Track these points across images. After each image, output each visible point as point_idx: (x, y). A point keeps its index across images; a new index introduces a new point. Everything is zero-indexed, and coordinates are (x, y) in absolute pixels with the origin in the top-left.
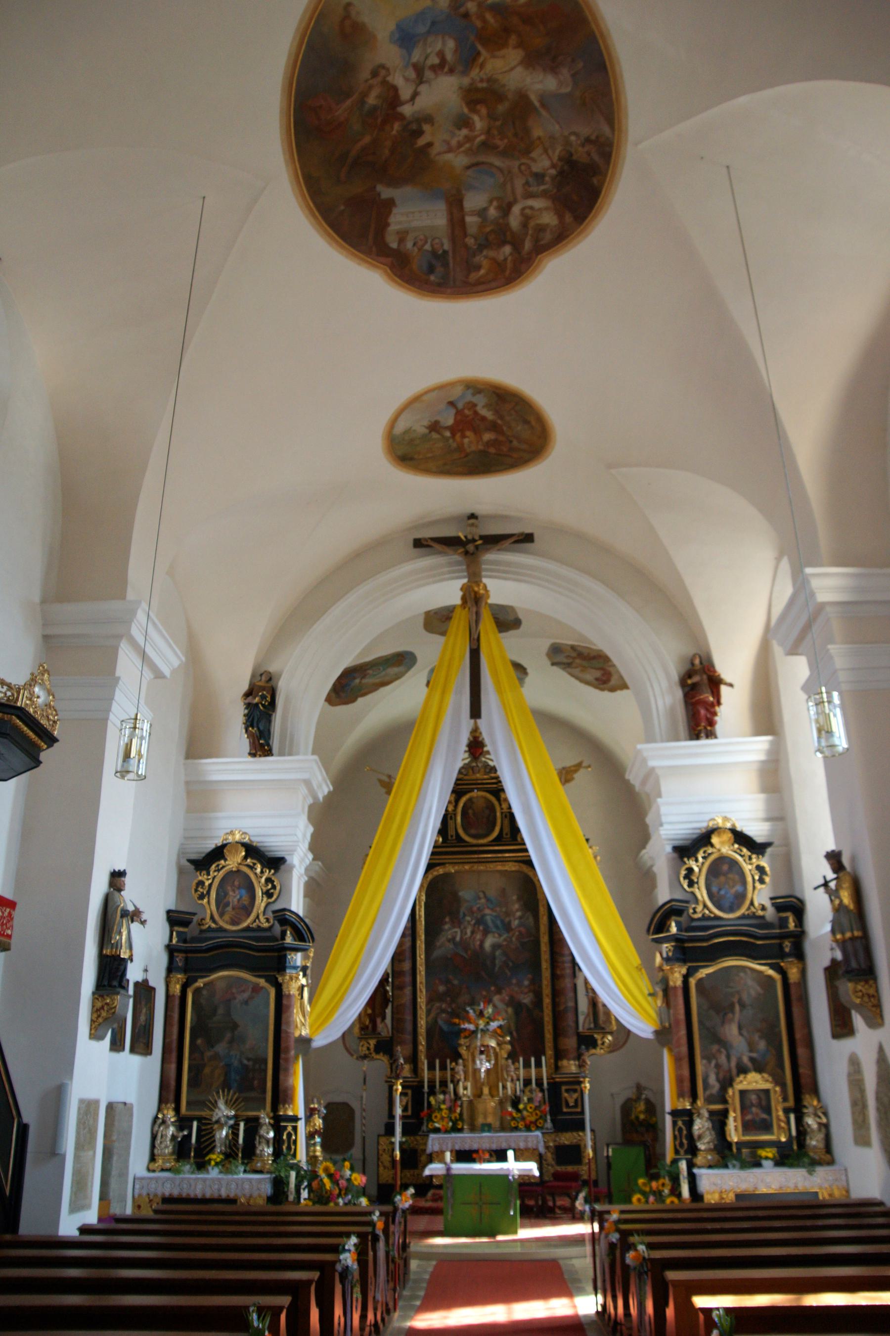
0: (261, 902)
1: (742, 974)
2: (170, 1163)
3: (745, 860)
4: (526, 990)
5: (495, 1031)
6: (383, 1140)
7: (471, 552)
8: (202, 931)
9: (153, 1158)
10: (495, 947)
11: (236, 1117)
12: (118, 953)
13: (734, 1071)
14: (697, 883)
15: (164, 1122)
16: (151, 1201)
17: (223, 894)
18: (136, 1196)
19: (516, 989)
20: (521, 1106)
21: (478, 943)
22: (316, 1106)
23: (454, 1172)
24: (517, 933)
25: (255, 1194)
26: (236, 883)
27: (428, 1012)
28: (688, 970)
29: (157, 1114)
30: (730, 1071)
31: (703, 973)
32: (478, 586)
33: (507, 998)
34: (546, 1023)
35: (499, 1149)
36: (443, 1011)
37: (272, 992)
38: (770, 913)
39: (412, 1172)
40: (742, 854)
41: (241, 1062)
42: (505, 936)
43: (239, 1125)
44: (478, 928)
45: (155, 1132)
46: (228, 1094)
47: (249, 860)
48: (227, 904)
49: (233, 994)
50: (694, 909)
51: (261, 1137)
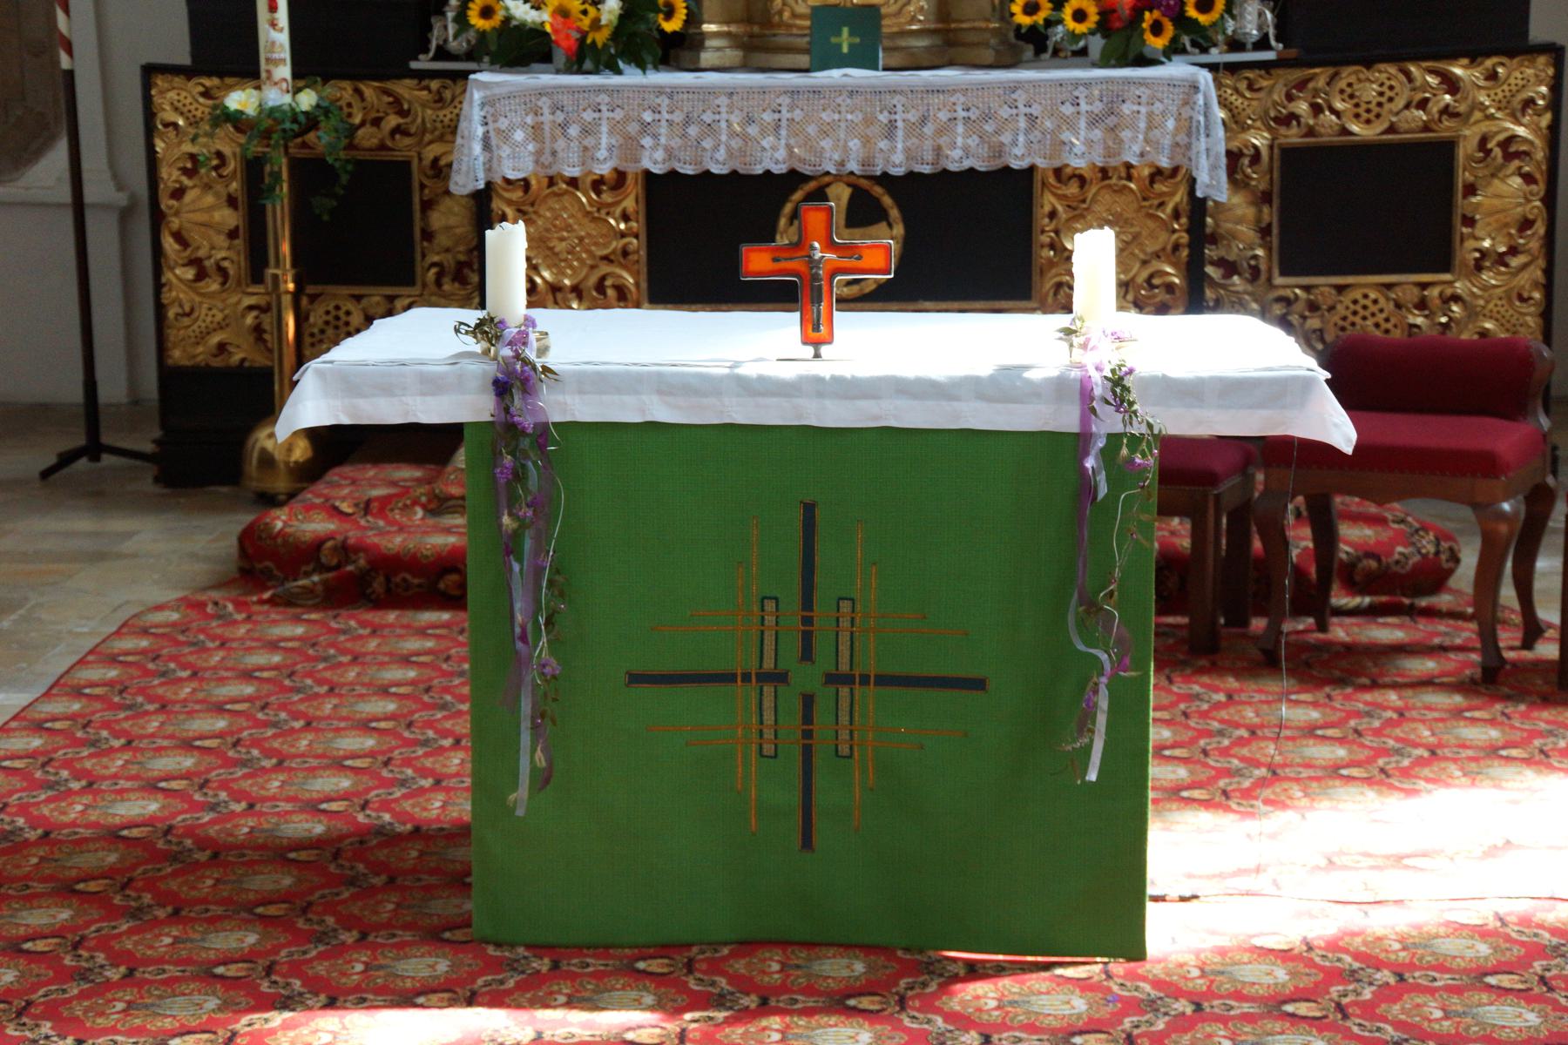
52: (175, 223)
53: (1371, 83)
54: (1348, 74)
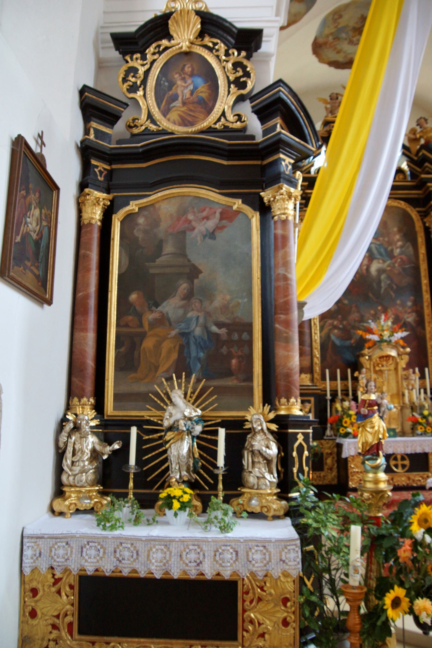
2: (90, 498)
4: (409, 310)
5: (396, 342)
10: (380, 271)
11: (202, 419)
15: (77, 428)
16: (57, 581)
17: (166, 84)
18: (27, 571)
19: (400, 309)
24: (399, 260)
25: (276, 572)
26: (188, 69)
27: (322, 329)
29: (65, 415)
35: (413, 452)
36: (335, 327)
41: (206, 328)
42: (389, 262)
43: (216, 433)
45: (61, 445)
46: (188, 380)
48: (175, 98)
49: (190, 222)
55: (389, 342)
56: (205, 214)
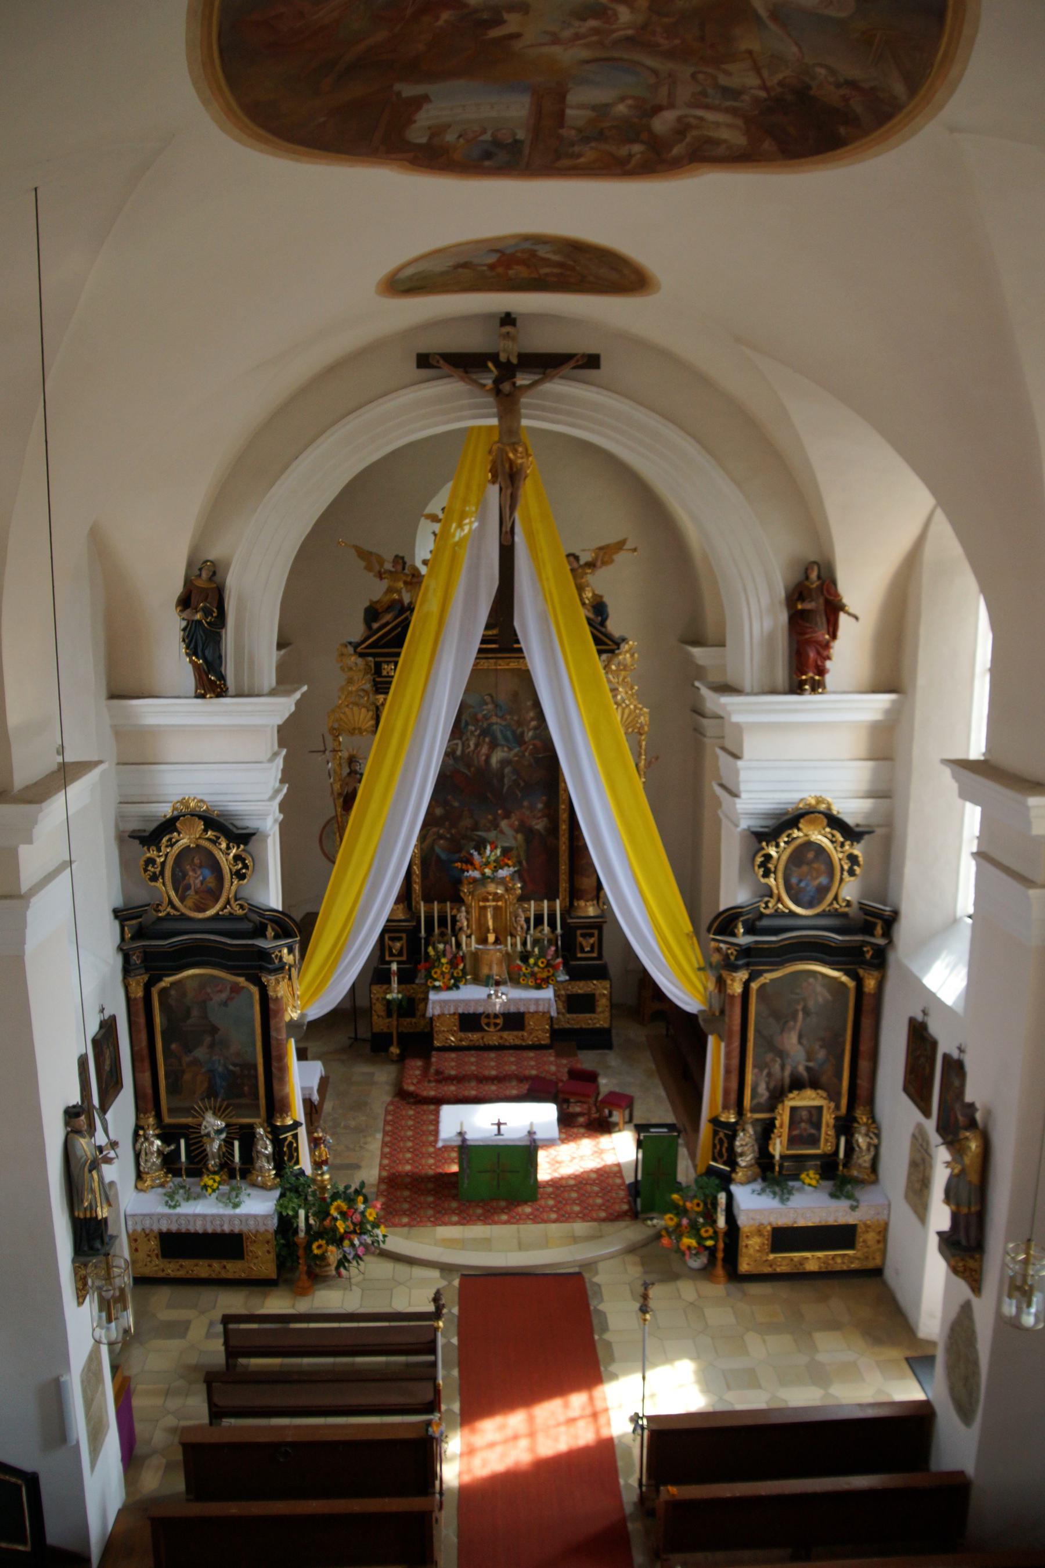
0: (231, 886)
1: (811, 980)
2: (159, 1178)
3: (835, 848)
6: (375, 989)
7: (507, 393)
8: (160, 919)
9: (139, 1176)
10: (504, 763)
11: (227, 1126)
12: (94, 1215)
13: (787, 1081)
14: (775, 873)
15: (146, 1139)
18: (130, 1231)
19: (528, 813)
20: (532, 961)
21: (483, 758)
22: (321, 1135)
23: (469, 1143)
24: (531, 747)
25: (262, 1229)
26: (197, 861)
28: (750, 974)
30: (782, 1079)
31: (767, 978)
32: (515, 451)
33: (516, 823)
34: (561, 853)
35: (506, 1011)
36: (441, 837)
37: (255, 990)
38: (852, 911)
39: (408, 1020)
40: (834, 839)
42: (516, 750)
44: (484, 741)
46: (216, 1101)
47: (209, 833)
48: (188, 887)
50: (767, 903)
51: (258, 1152)
52: (374, 1008)
53: (582, 984)
54: (578, 983)
55: (493, 879)
56: (219, 988)
